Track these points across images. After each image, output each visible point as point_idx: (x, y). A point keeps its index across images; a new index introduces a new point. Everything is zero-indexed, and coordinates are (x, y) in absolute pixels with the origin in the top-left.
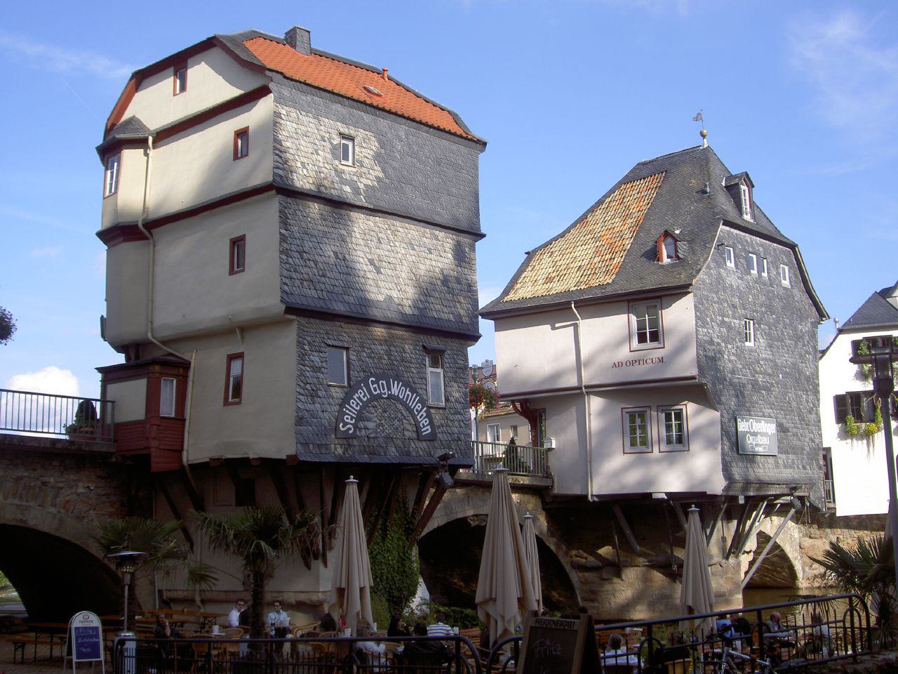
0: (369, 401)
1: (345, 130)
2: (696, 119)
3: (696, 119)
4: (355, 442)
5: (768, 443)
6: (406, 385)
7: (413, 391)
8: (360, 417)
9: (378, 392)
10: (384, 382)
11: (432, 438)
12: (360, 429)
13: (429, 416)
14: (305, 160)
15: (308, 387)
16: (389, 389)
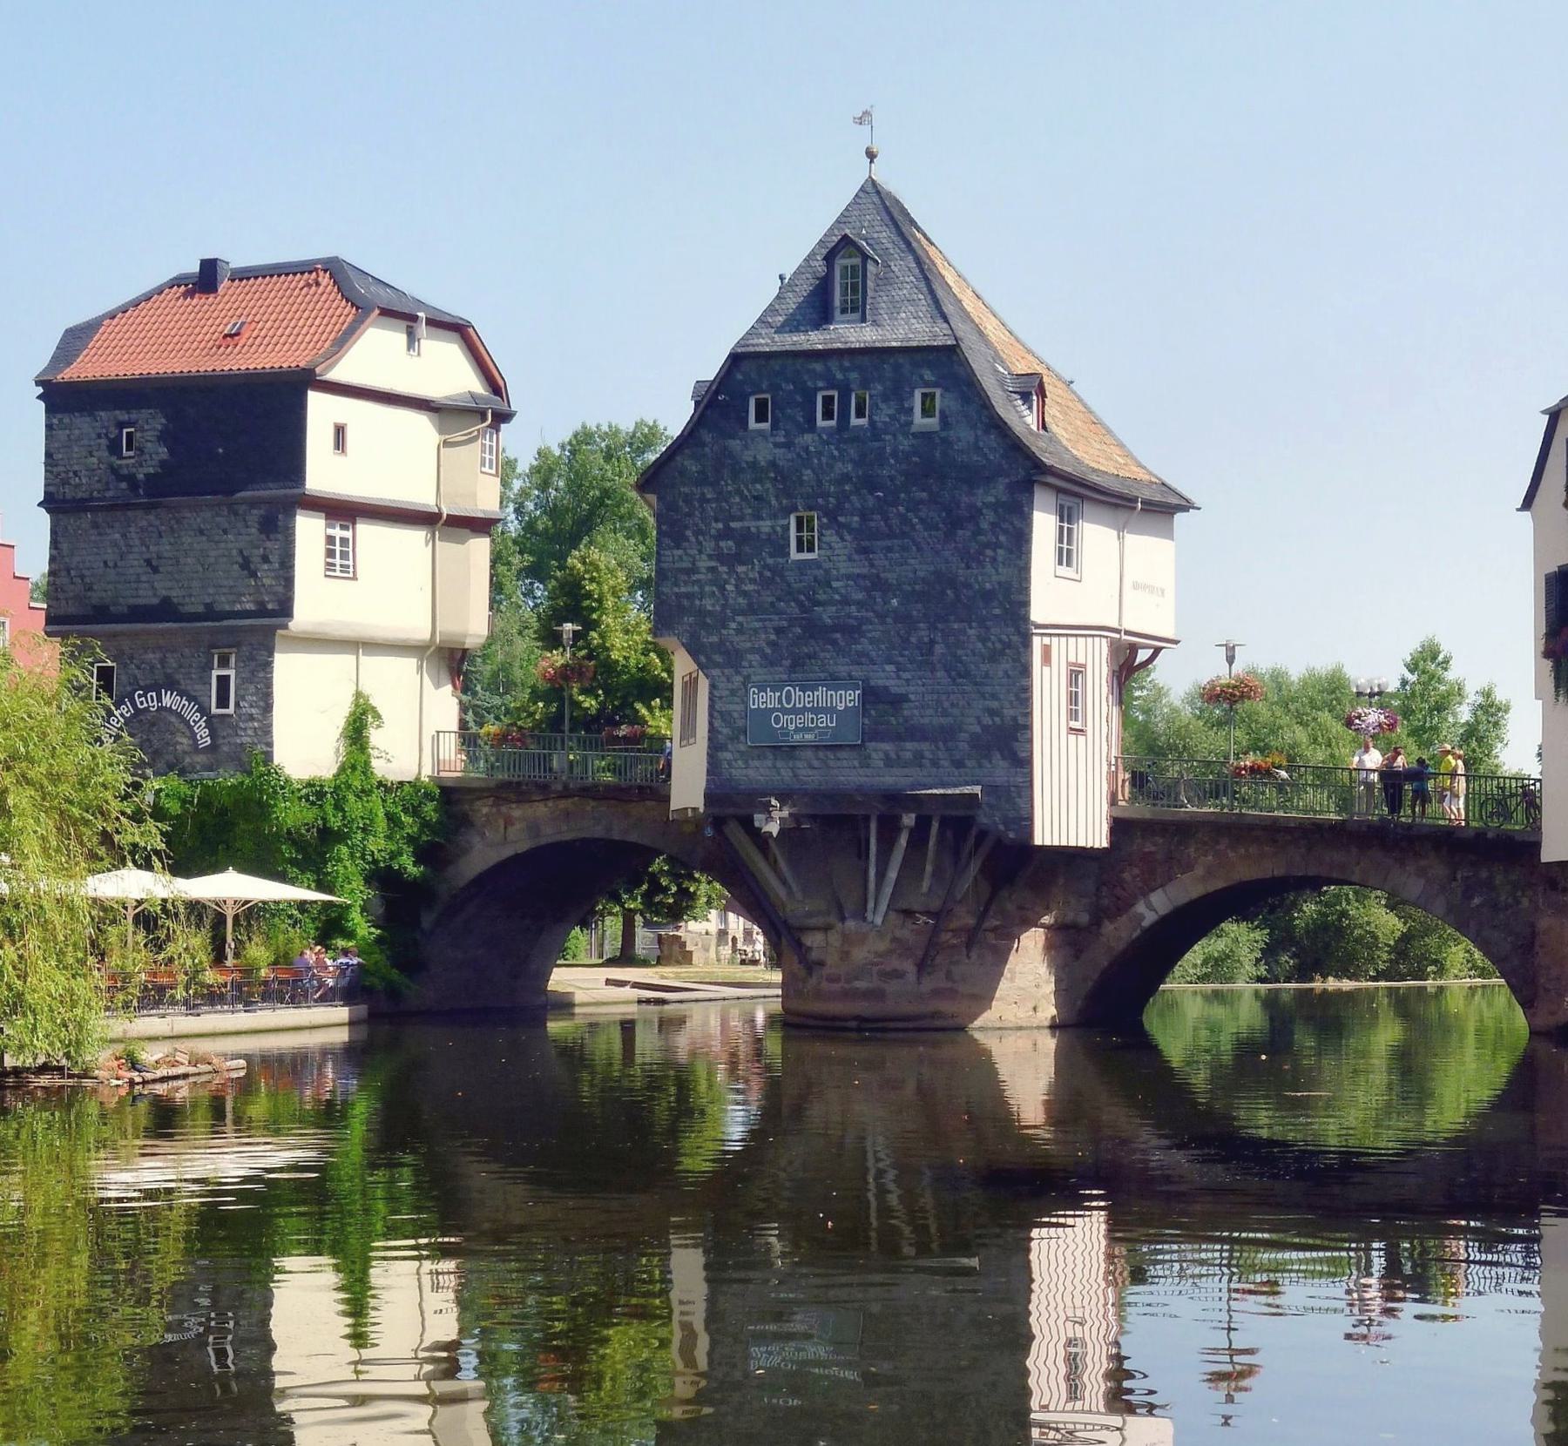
2: (860, 121)
3: (860, 121)
11: (213, 748)
13: (209, 725)
14: (76, 468)
16: (159, 700)
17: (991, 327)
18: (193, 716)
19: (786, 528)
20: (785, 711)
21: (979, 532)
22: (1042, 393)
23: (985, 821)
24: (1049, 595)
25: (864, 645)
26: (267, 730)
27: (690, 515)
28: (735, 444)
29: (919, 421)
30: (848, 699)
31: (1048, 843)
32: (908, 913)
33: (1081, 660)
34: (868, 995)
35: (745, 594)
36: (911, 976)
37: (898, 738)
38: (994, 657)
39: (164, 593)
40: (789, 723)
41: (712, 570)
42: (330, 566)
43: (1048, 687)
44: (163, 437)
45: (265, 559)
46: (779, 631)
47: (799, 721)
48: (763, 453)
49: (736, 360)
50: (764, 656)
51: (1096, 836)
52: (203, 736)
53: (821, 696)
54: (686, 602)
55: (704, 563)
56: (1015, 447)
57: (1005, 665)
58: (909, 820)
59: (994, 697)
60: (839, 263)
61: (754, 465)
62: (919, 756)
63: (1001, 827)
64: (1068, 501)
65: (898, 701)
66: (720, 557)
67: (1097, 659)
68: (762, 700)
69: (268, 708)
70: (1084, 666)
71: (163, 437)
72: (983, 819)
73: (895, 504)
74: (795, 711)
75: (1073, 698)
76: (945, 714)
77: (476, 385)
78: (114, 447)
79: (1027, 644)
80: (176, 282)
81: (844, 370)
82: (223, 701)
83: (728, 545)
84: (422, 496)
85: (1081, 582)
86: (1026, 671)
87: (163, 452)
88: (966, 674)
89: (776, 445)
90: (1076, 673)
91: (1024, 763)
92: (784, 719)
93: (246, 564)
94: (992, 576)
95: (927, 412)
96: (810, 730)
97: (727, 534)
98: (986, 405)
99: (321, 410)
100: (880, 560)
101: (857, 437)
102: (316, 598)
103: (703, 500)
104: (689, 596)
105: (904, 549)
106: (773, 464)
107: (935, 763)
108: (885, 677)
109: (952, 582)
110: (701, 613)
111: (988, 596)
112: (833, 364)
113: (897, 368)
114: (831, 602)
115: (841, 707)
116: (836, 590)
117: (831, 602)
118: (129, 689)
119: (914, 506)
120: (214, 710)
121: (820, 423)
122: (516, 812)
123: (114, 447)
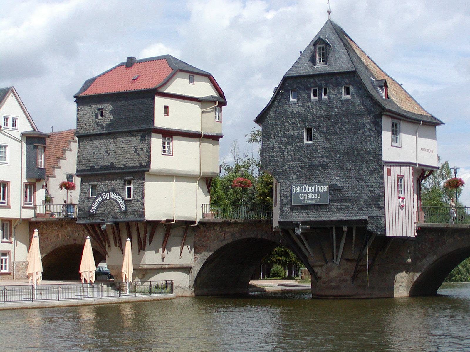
0: (102, 201)
1: (99, 106)
4: (96, 216)
5: (320, 197)
6: (116, 193)
7: (119, 195)
8: (98, 207)
9: (106, 197)
10: (108, 194)
12: (98, 211)
13: (125, 203)
14: (86, 123)
15: (82, 199)
16: (110, 196)
17: (371, 66)
18: (119, 200)
19: (303, 133)
20: (304, 193)
21: (365, 132)
22: (387, 87)
23: (370, 228)
24: (389, 153)
25: (329, 170)
26: (143, 204)
27: (272, 130)
28: (286, 107)
29: (345, 97)
30: (324, 188)
31: (391, 235)
32: (347, 260)
33: (402, 174)
34: (335, 288)
35: (291, 155)
36: (350, 282)
37: (341, 201)
38: (371, 173)
39: (112, 161)
40: (305, 197)
41: (279, 147)
42: (164, 151)
43: (390, 183)
44: (112, 112)
45: (142, 149)
46: (302, 167)
47: (309, 196)
48: (295, 109)
49: (285, 79)
50: (296, 175)
51: (412, 233)
52: (123, 208)
53: (316, 188)
54: (271, 158)
55: (277, 145)
56: (376, 103)
57: (375, 175)
58: (345, 229)
59: (372, 186)
60: (318, 46)
61: (292, 113)
62: (347, 207)
63: (375, 230)
64: (395, 121)
65: (341, 189)
66: (282, 143)
67: (408, 173)
68: (296, 190)
69: (143, 197)
70: (404, 176)
71: (112, 112)
72: (369, 228)
73: (337, 123)
74: (307, 193)
75: (399, 186)
76: (356, 193)
77: (215, 94)
78: (97, 116)
79: (382, 169)
80: (121, 65)
81: (320, 80)
82: (129, 196)
83: (285, 139)
84: (196, 128)
85: (401, 148)
86: (382, 178)
87: (111, 117)
88: (362, 179)
89: (299, 106)
90: (400, 178)
91: (382, 208)
92: (304, 196)
93: (136, 152)
94: (369, 147)
95: (348, 93)
96: (312, 199)
97: (284, 136)
98: (366, 90)
99: (159, 102)
100: (333, 142)
101: (324, 103)
102: (158, 162)
103: (276, 125)
104: (272, 156)
105: (341, 138)
106: (298, 112)
107: (353, 209)
108: (336, 181)
109: (357, 150)
110: (276, 162)
111: (368, 153)
112: (317, 79)
113: (337, 79)
114: (318, 157)
115: (322, 191)
116: (319, 153)
117: (318, 157)
118: (101, 192)
119: (344, 124)
120: (126, 198)
121: (313, 97)
122: (228, 230)
123: (97, 116)
